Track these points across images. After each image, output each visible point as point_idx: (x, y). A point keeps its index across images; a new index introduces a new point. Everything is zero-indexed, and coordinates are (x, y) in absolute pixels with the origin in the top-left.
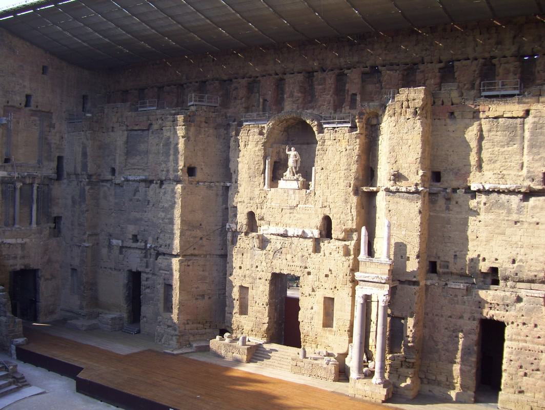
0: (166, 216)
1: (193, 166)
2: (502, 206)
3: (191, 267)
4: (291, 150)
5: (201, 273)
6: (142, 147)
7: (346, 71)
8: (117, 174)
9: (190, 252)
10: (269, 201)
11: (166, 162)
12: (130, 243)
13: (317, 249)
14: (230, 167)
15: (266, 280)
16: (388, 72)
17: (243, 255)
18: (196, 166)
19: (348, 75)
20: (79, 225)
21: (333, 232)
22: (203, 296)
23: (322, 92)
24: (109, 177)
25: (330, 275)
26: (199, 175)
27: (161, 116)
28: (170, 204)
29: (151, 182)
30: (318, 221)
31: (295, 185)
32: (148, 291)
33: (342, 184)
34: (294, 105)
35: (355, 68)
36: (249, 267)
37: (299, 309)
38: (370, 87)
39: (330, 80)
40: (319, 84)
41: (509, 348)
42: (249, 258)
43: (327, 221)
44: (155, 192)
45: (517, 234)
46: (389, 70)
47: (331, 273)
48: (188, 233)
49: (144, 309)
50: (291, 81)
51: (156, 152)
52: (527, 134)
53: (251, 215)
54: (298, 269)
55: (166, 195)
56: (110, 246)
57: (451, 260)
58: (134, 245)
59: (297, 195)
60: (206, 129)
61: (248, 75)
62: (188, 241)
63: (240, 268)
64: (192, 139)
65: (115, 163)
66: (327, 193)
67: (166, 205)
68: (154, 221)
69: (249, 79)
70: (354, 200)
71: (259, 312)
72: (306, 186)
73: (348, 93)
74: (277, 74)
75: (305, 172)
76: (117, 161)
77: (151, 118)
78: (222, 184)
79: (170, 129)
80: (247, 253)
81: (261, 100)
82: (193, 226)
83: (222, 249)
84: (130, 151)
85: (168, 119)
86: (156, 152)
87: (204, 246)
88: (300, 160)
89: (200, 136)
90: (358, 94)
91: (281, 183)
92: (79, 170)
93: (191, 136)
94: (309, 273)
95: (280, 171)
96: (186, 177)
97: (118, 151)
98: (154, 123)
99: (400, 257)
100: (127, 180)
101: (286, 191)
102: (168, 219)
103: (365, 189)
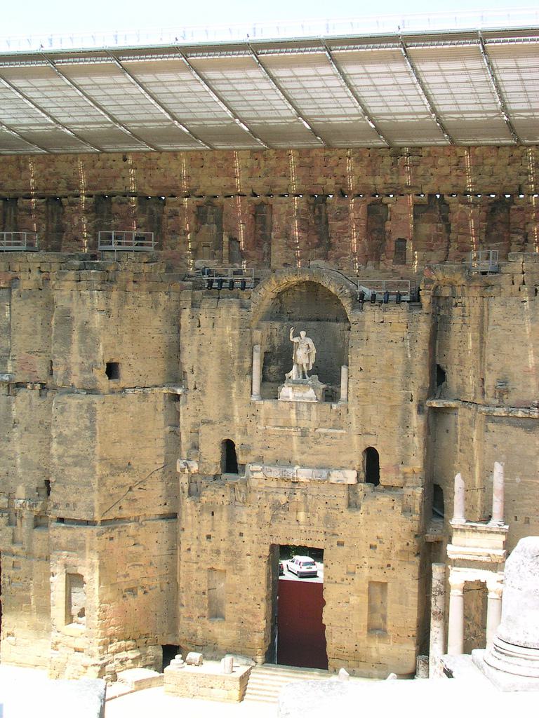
0: (66, 451)
1: (114, 361)
3: (116, 540)
4: (300, 336)
5: (134, 548)
7: (385, 200)
9: (115, 513)
10: (262, 421)
11: (65, 353)
13: (353, 505)
14: (183, 360)
15: (260, 557)
16: (461, 206)
17: (213, 514)
18: (120, 361)
19: (389, 206)
21: (381, 474)
22: (132, 591)
23: (342, 233)
26: (126, 376)
27: (38, 265)
28: (76, 429)
30: (358, 459)
34: (290, 251)
35: (403, 195)
36: (224, 535)
37: (324, 603)
38: (426, 229)
40: (337, 219)
42: (224, 518)
43: (371, 456)
44: (30, 403)
46: (462, 204)
48: (109, 481)
50: (282, 209)
51: (30, 330)
53: (229, 446)
54: (321, 536)
55: (65, 414)
59: (314, 413)
60: (136, 294)
61: (197, 193)
62: (111, 495)
63: (209, 537)
64: (114, 312)
66: (371, 410)
67: (67, 432)
68: (29, 457)
69: (200, 199)
70: (417, 421)
71: (247, 612)
72: (331, 396)
73: (389, 237)
74: (255, 195)
75: (327, 374)
77: (17, 268)
78: (165, 390)
79: (72, 296)
81: (226, 239)
82: (119, 468)
83: (166, 504)
85: (66, 277)
86: (30, 330)
87: (136, 500)
88: (315, 352)
89: (127, 307)
90: (408, 240)
91: (287, 392)
93: (113, 308)
94: (340, 544)
95: (272, 366)
96: (104, 383)
98: (22, 276)
99: (514, 518)
102: (73, 456)
103: (435, 404)
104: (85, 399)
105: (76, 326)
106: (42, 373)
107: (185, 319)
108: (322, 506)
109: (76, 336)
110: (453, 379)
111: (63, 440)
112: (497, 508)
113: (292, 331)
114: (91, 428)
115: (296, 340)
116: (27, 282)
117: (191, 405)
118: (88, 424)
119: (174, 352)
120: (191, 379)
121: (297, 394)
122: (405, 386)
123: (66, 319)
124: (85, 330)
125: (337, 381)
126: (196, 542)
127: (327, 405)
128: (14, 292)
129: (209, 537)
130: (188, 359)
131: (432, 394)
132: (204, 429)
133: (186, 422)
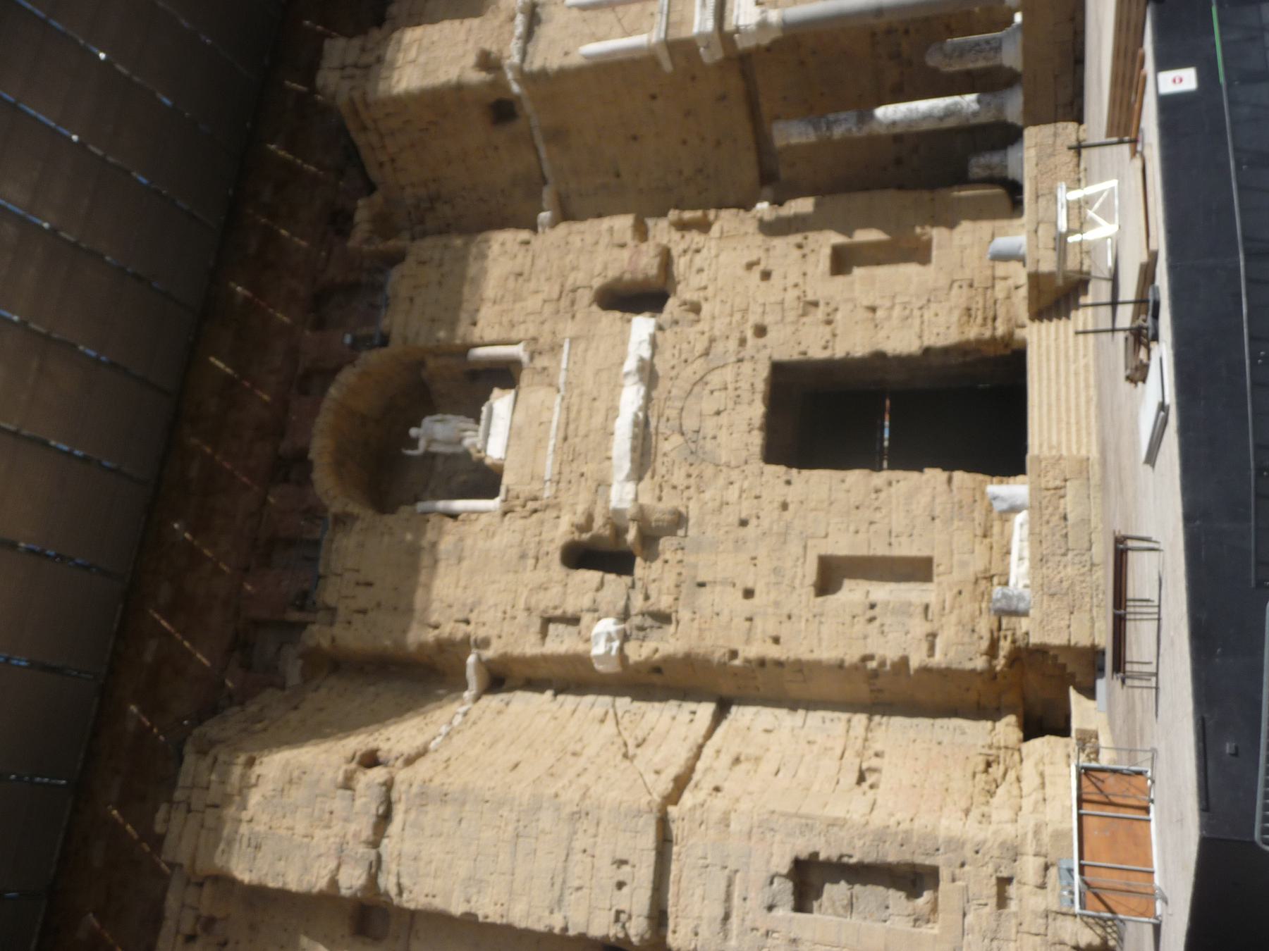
15: (788, 483)
17: (702, 585)
25: (761, 267)
27: (180, 939)
31: (501, 403)
47: (757, 263)
53: (580, 556)
54: (747, 367)
66: (533, 303)
80: (695, 566)
91: (495, 450)
101: (514, 433)
102: (514, 854)
108: (690, 369)
111: (475, 882)
113: (410, 452)
115: (422, 444)
118: (448, 811)
126: (758, 621)
127: (525, 378)
129: (749, 594)
133: (529, 646)
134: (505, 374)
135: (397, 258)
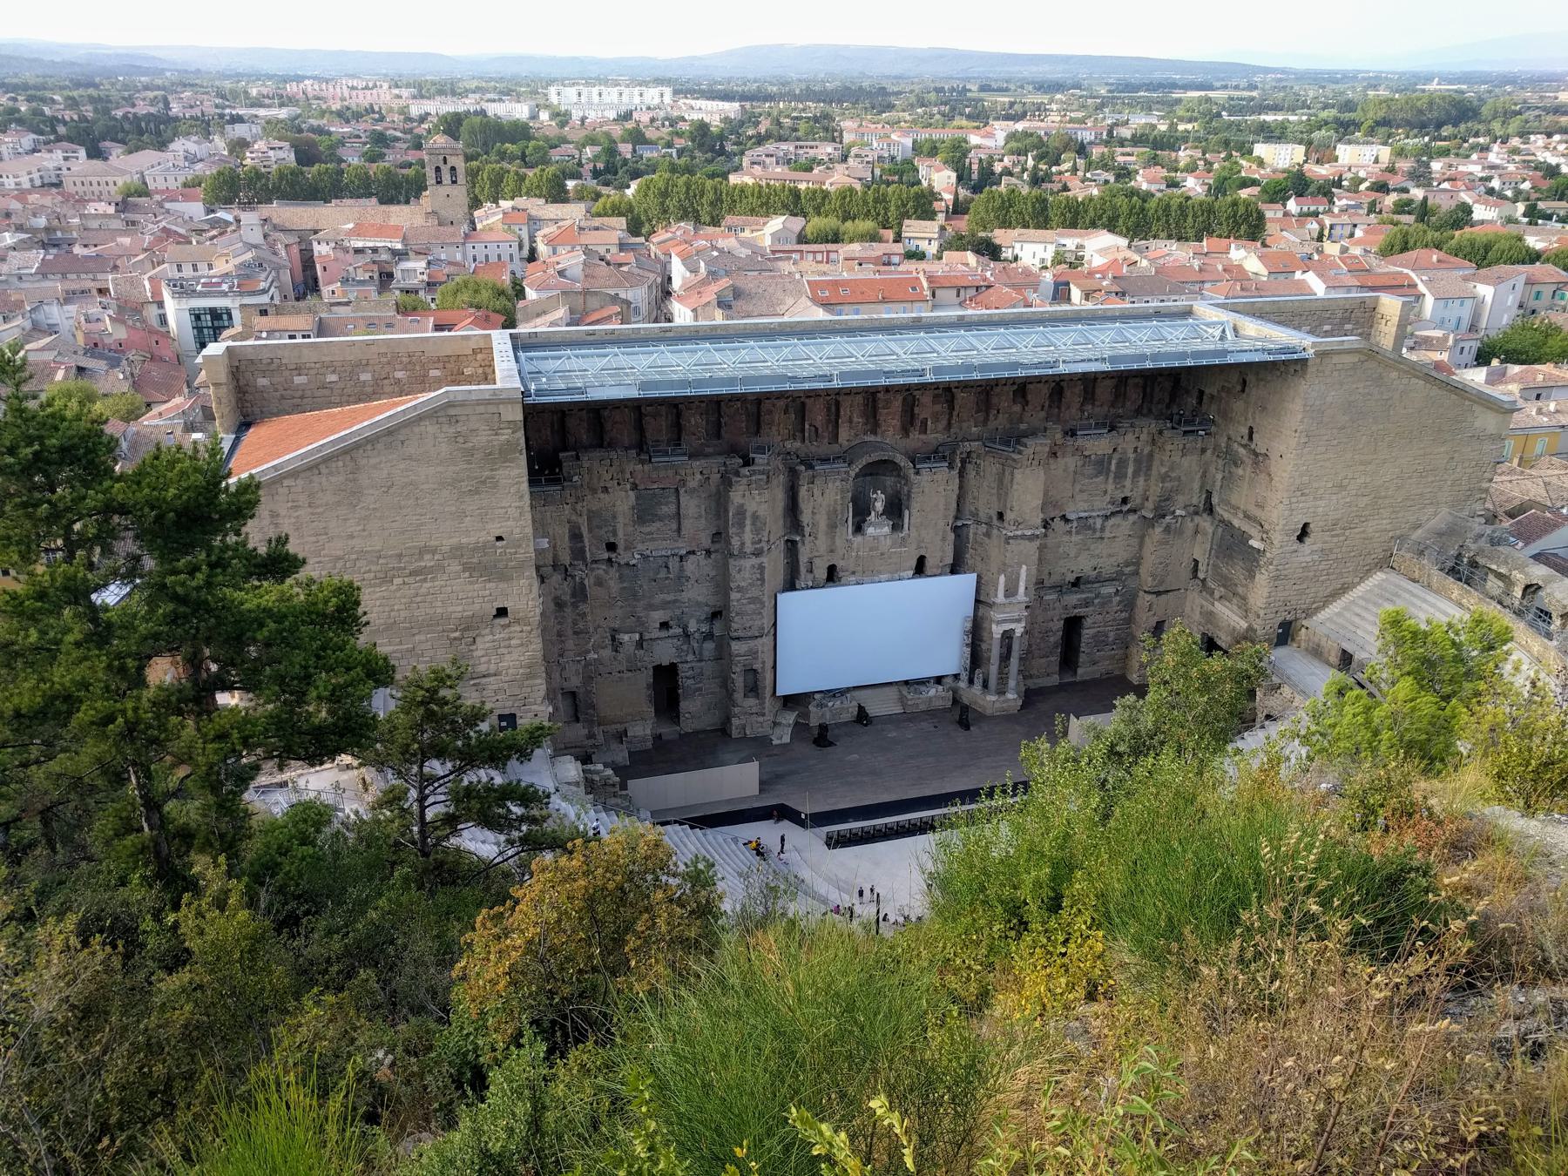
2: (1089, 528)
6: (668, 509)
8: (620, 549)
12: (656, 634)
20: (575, 633)
24: (606, 555)
29: (693, 553)
30: (914, 563)
31: (887, 530)
32: (690, 682)
33: (941, 523)
38: (938, 407)
39: (897, 403)
41: (1087, 633)
45: (1099, 548)
49: (686, 706)
52: (1113, 467)
56: (616, 645)
57: (1046, 577)
58: (664, 634)
65: (615, 533)
76: (620, 534)
84: (644, 513)
91: (870, 530)
92: (566, 558)
97: (620, 519)
100: (645, 557)
103: (959, 523)
104: (754, 561)
105: (748, 514)
106: (706, 542)
107: (803, 492)
109: (748, 522)
110: (969, 507)
111: (740, 589)
112: (1022, 590)
114: (762, 580)
116: (693, 483)
117: (808, 546)
119: (793, 508)
120: (807, 530)
121: (877, 529)
122: (946, 517)
123: (741, 512)
124: (755, 517)
125: (900, 516)
127: (895, 536)
128: (682, 491)
130: (806, 518)
131: (957, 518)
132: (817, 562)
134: (896, 527)
135: (951, 467)
